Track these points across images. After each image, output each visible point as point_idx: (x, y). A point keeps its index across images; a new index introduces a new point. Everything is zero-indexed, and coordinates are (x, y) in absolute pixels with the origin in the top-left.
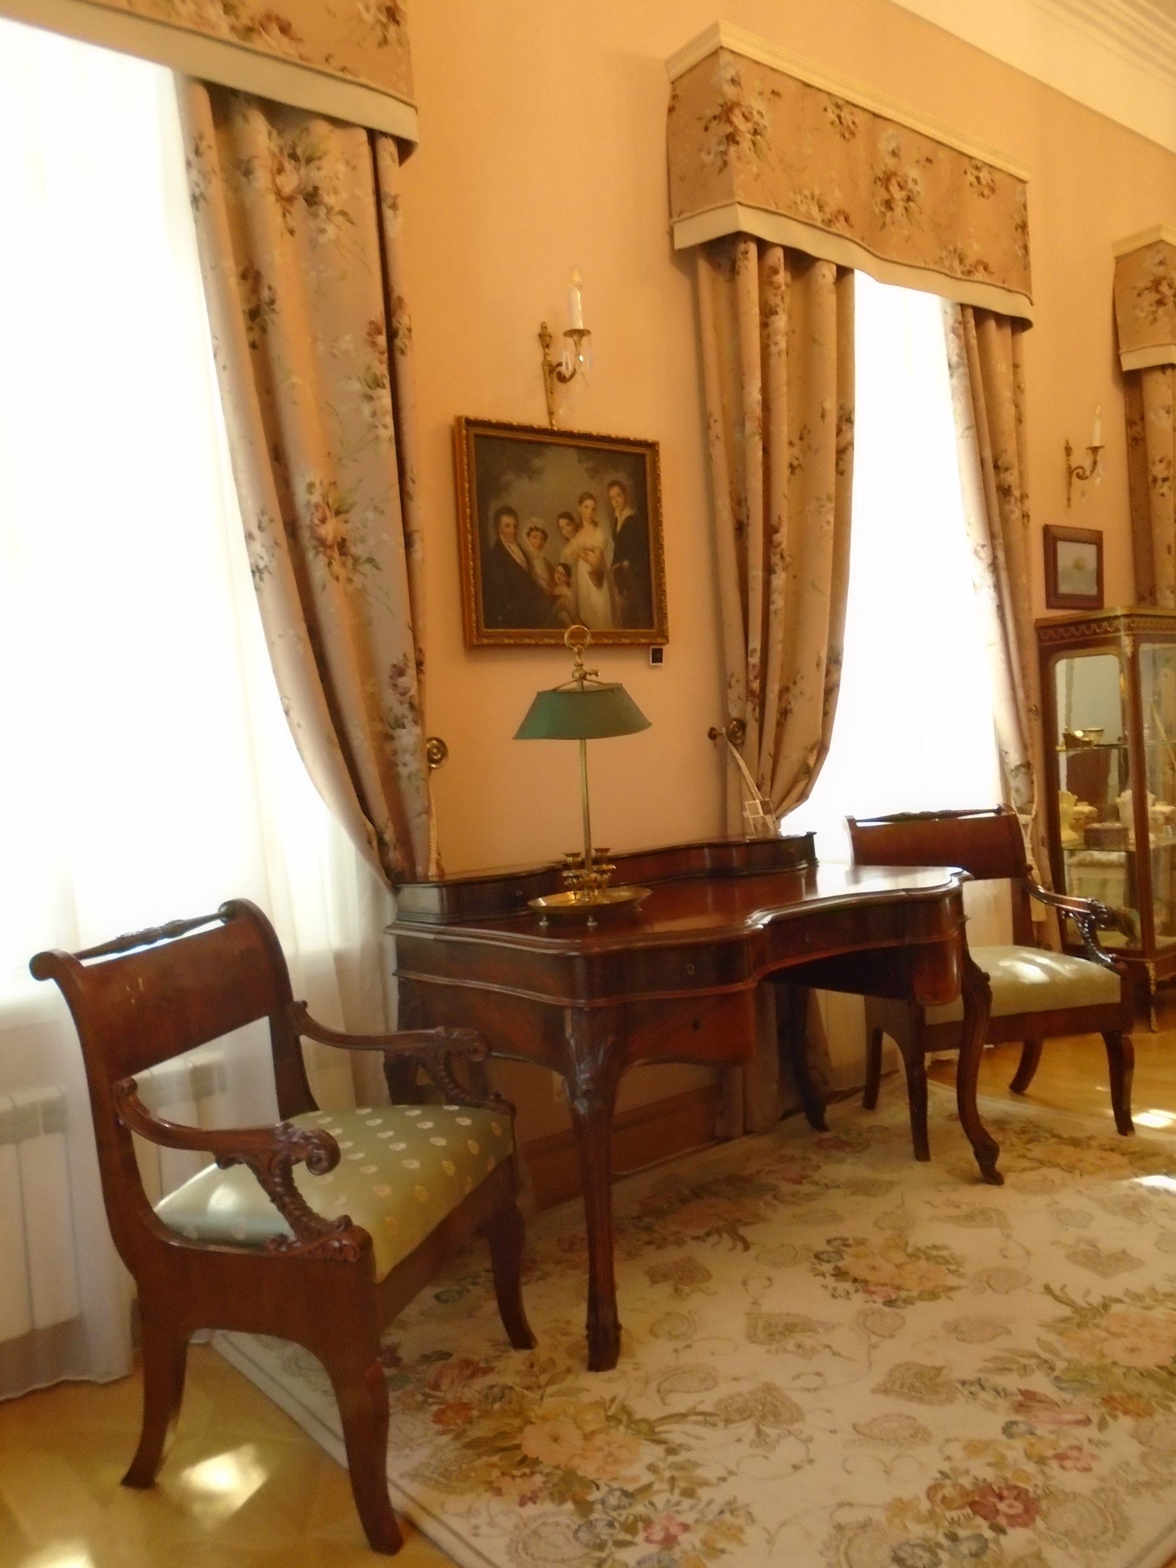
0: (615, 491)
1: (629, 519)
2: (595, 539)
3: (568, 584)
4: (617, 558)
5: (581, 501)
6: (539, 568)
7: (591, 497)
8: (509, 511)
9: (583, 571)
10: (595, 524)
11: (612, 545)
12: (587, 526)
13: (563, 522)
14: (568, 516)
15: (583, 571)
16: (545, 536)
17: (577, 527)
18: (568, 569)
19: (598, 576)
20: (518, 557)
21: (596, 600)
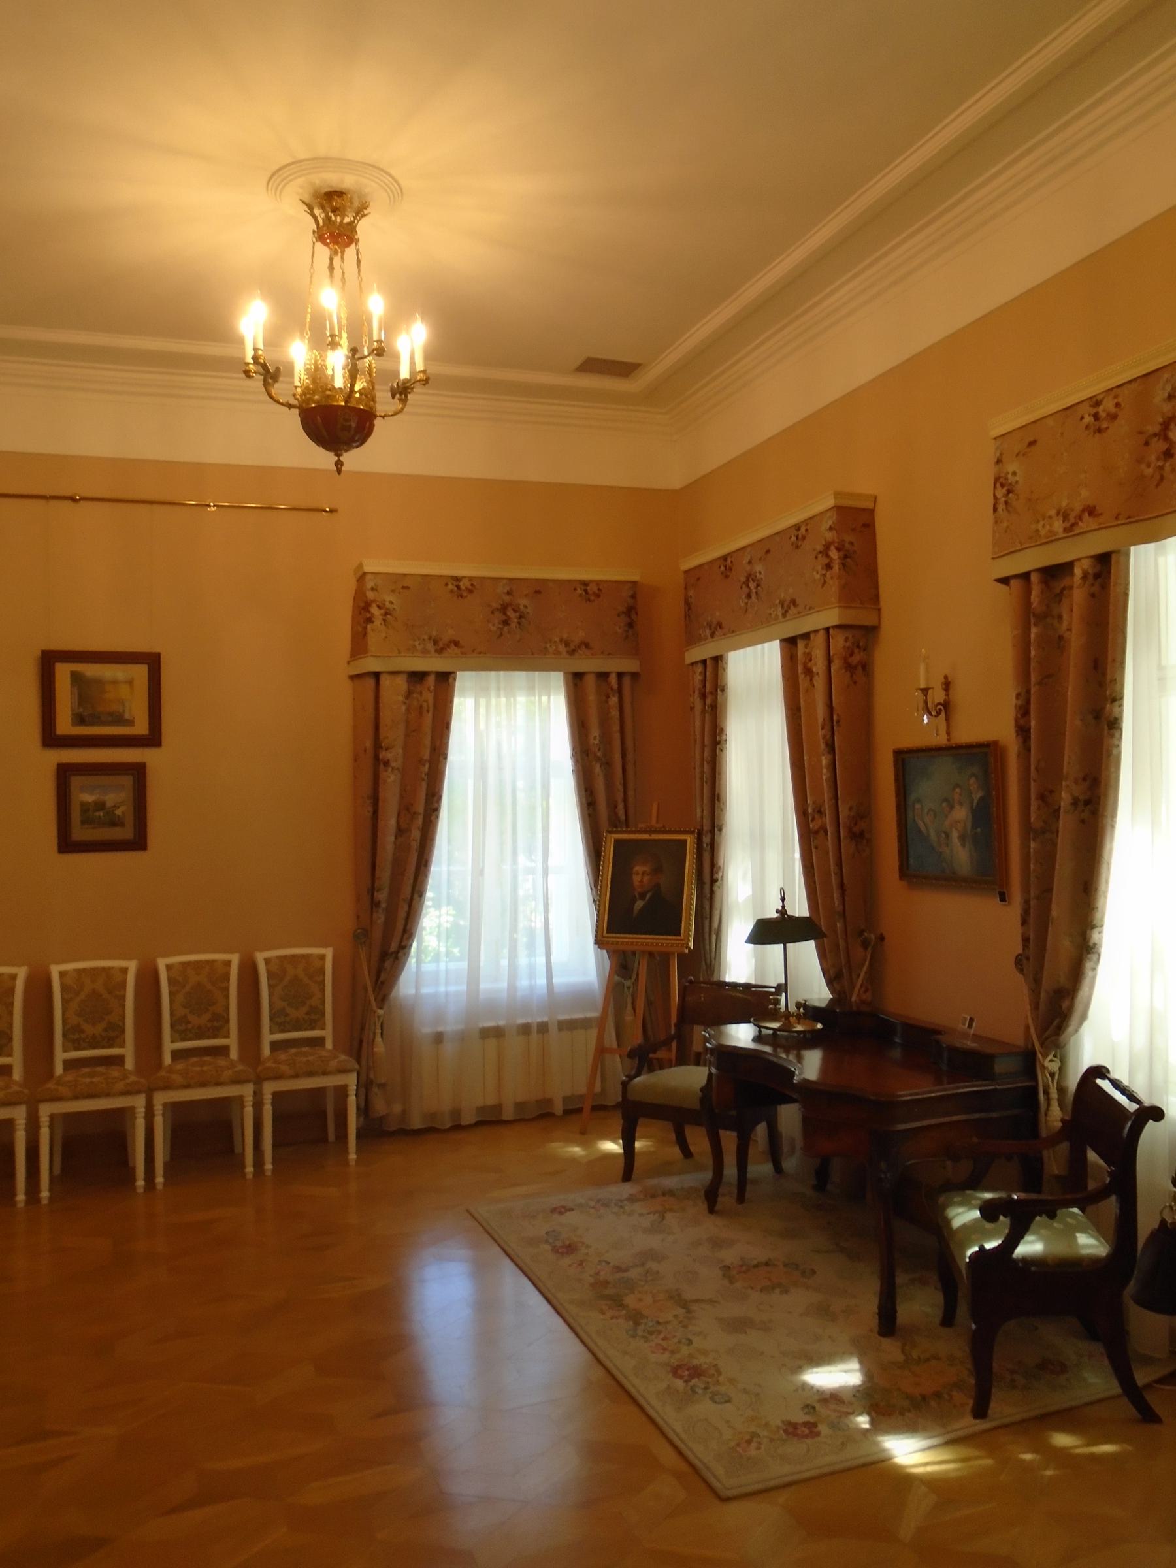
0: (973, 780)
1: (982, 799)
2: (961, 814)
3: (947, 845)
4: (974, 826)
5: (954, 789)
6: (933, 834)
7: (958, 786)
8: (919, 801)
9: (955, 835)
10: (961, 804)
11: (970, 817)
12: (957, 807)
13: (944, 804)
14: (946, 800)
15: (955, 835)
16: (935, 815)
17: (952, 807)
18: (947, 836)
19: (962, 838)
20: (923, 829)
21: (961, 856)
